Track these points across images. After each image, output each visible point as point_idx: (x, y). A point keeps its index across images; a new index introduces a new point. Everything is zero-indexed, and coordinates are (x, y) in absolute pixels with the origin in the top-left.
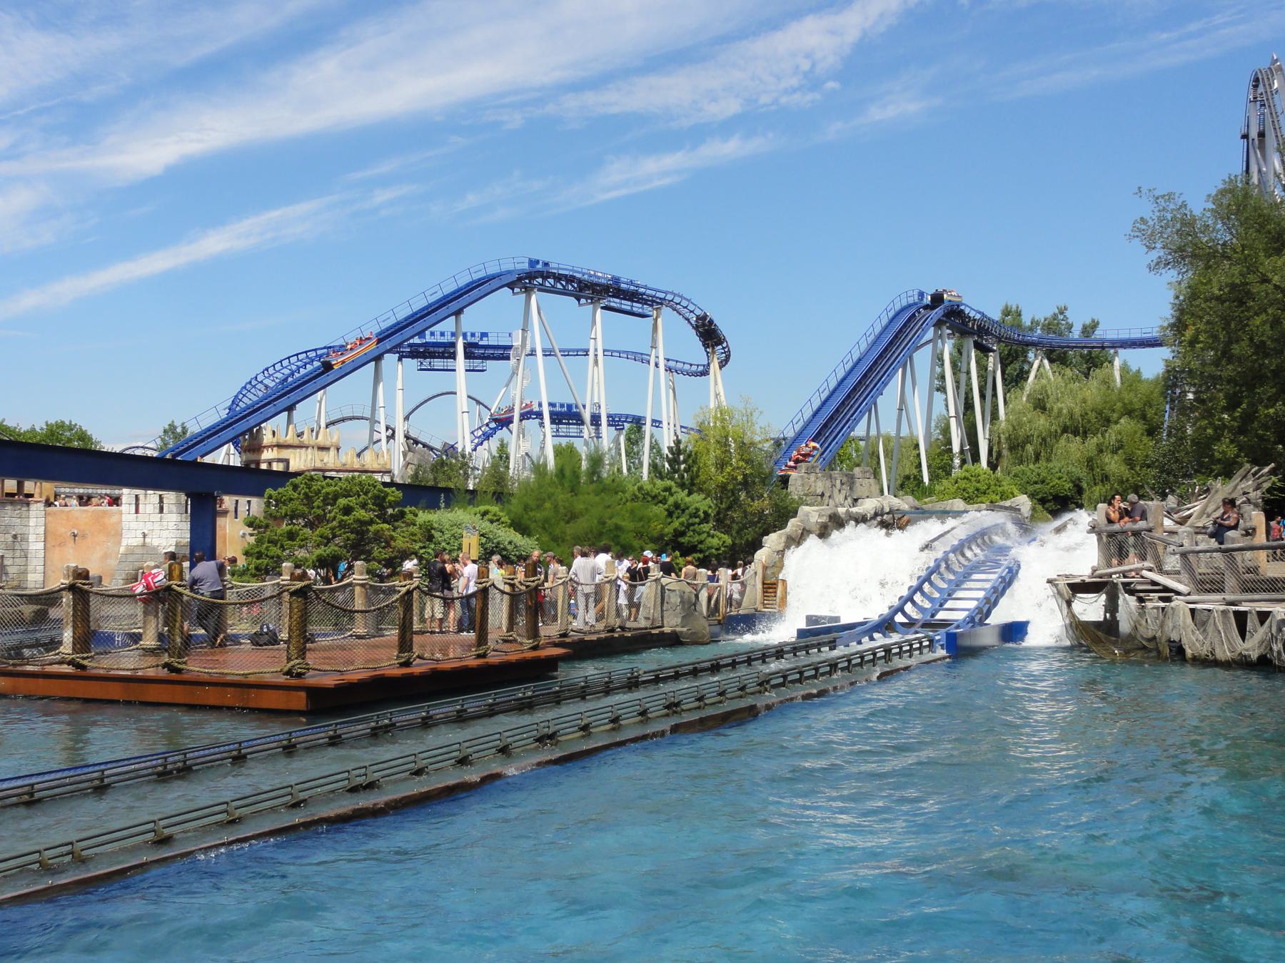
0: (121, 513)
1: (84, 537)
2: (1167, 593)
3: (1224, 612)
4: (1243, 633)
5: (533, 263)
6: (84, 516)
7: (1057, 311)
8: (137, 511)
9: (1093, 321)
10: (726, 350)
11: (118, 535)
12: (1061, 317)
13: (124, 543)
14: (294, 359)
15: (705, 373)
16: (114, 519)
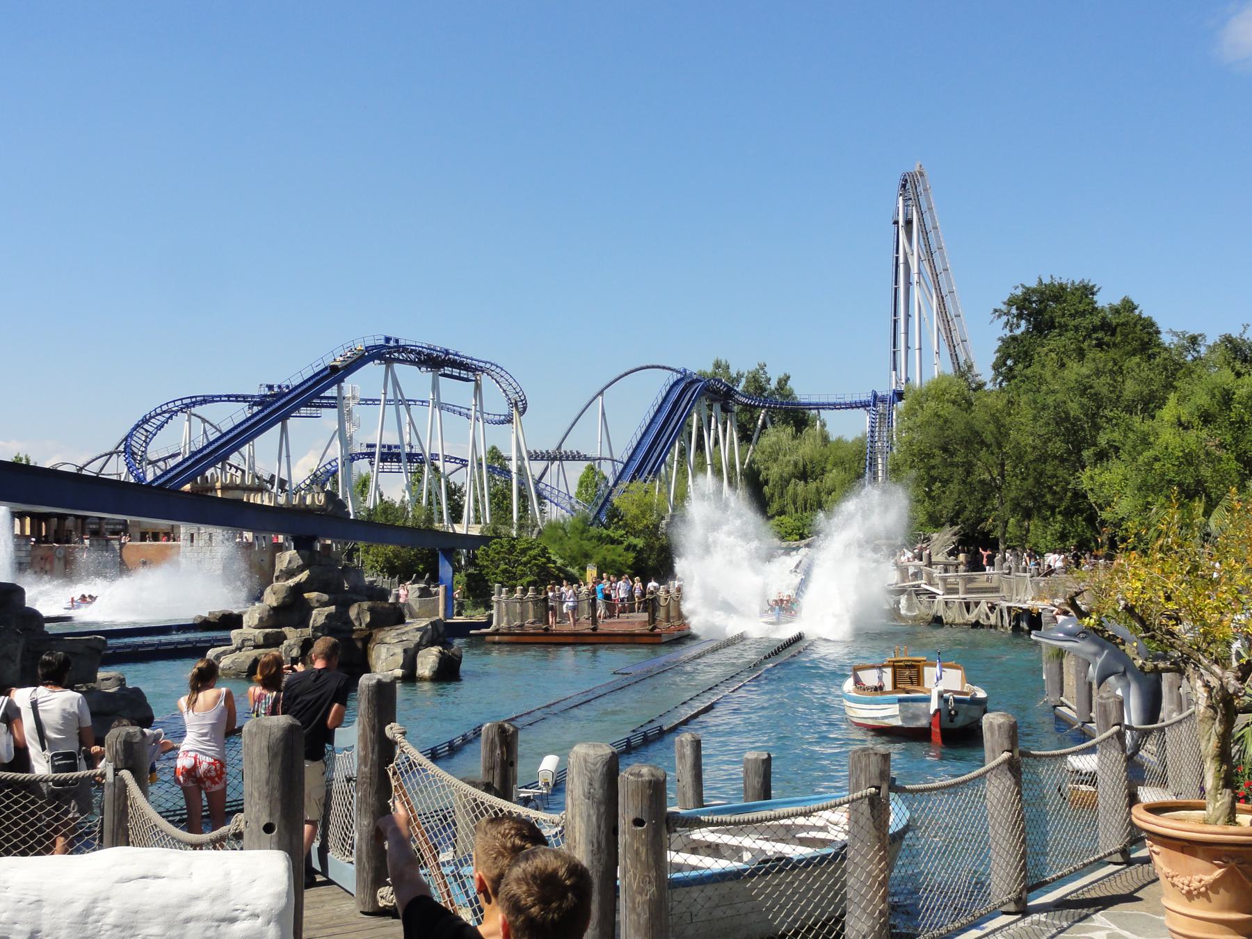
2: (932, 595)
3: (961, 602)
4: (968, 610)
5: (388, 340)
6: (150, 548)
7: (758, 367)
9: (785, 374)
12: (761, 372)
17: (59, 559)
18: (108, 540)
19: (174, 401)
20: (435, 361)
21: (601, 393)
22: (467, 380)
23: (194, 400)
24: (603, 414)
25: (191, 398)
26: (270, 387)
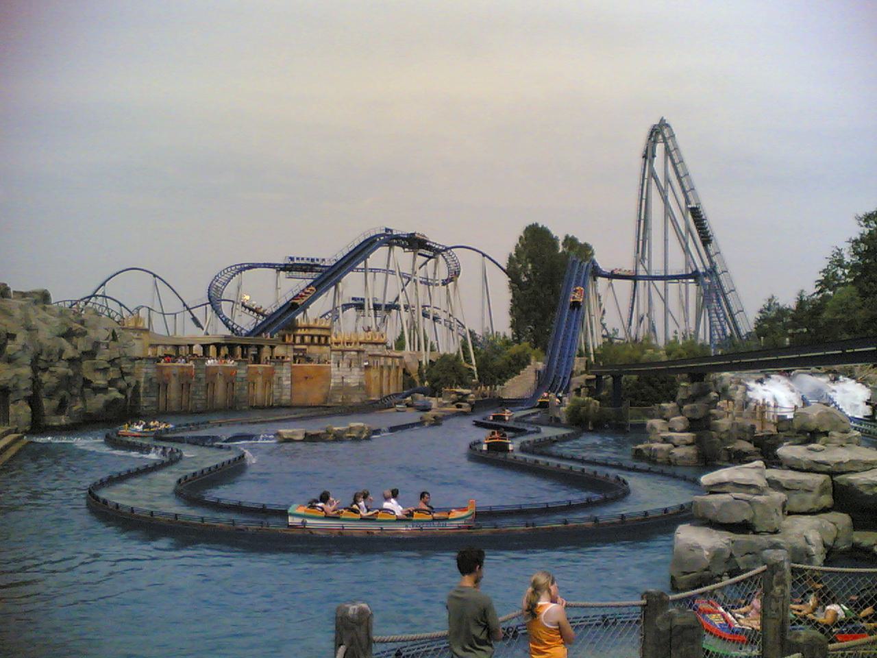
0: (330, 367)
8: (338, 366)
20: (415, 243)
26: (292, 259)
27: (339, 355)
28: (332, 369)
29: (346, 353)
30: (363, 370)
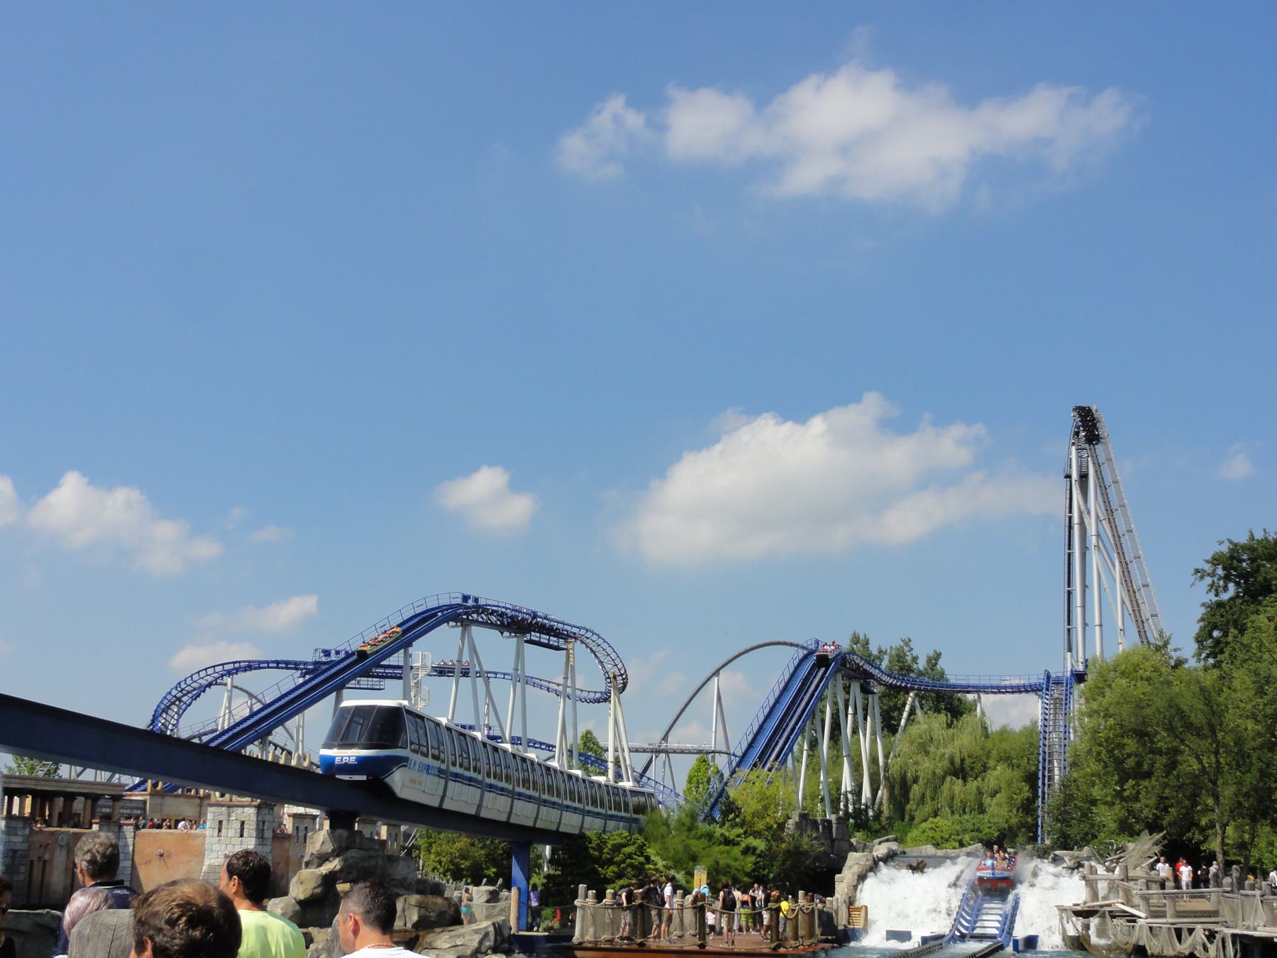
0: (204, 836)
1: (169, 856)
2: (1132, 919)
3: (1169, 929)
4: (1180, 940)
5: (466, 598)
7: (902, 644)
9: (935, 651)
10: (624, 677)
11: (201, 855)
13: (207, 862)
14: (202, 674)
15: (607, 700)
16: (198, 842)
17: (61, 847)
18: (120, 826)
19: (214, 667)
21: (717, 673)
22: (557, 648)
23: (237, 665)
24: (719, 698)
25: (234, 663)
26: (327, 653)
27: (221, 814)
28: (208, 840)
29: (235, 809)
30: (269, 842)
